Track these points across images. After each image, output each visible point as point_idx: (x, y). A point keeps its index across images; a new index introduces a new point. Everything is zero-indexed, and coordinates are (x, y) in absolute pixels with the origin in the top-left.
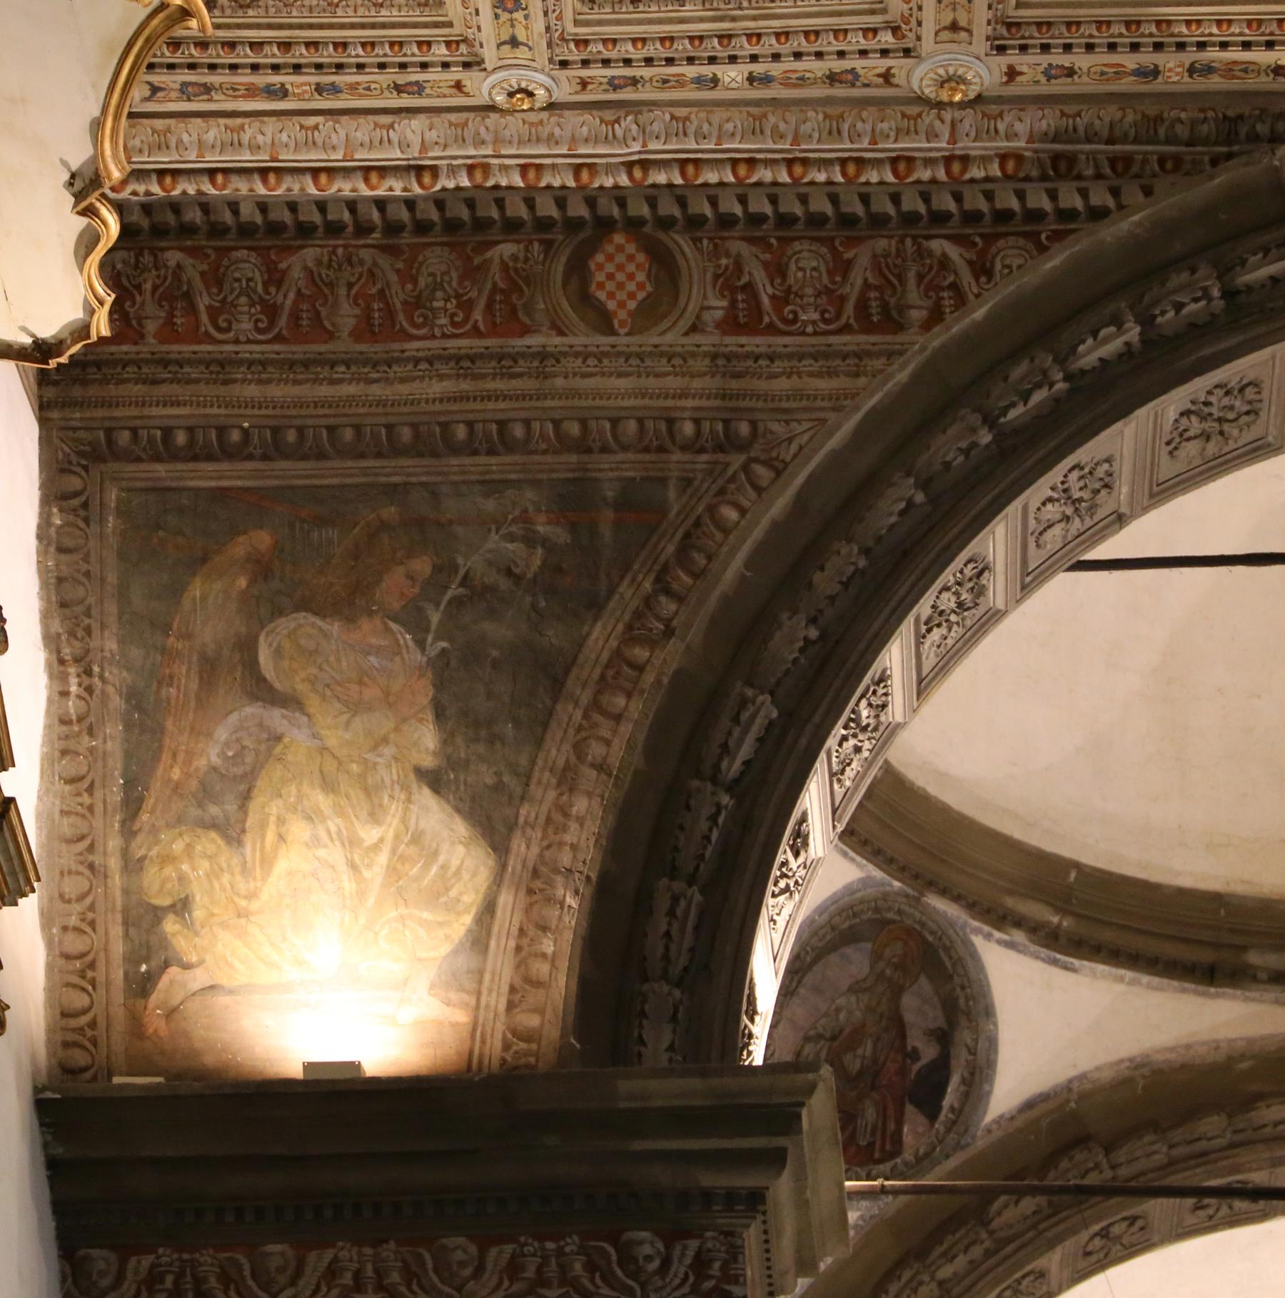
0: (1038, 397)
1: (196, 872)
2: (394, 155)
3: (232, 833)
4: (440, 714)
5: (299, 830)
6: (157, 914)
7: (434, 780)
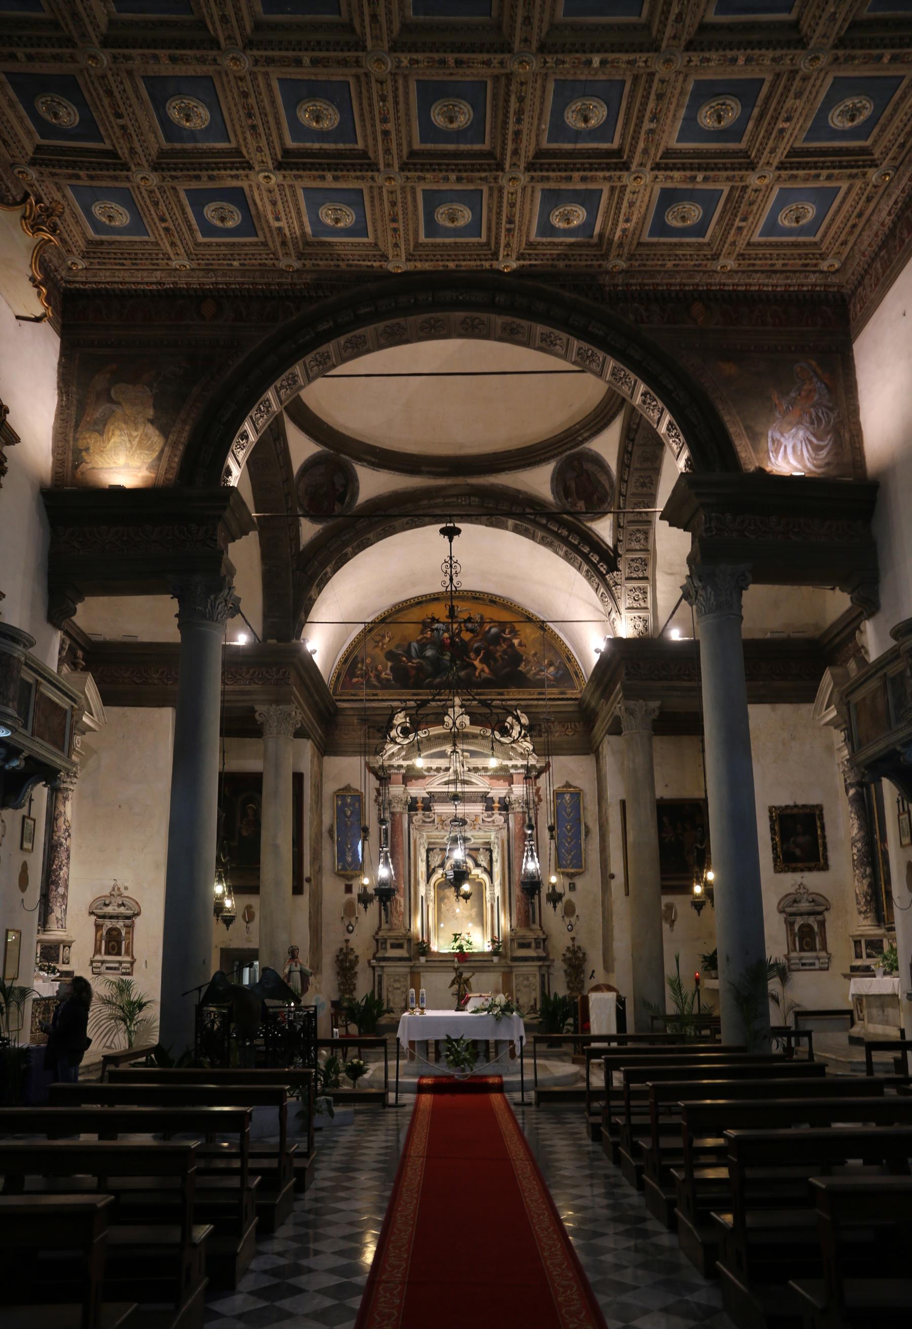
0: (307, 337)
1: (91, 442)
2: (154, 280)
3: (101, 433)
4: (155, 407)
5: (117, 432)
6: (81, 451)
7: (152, 422)
